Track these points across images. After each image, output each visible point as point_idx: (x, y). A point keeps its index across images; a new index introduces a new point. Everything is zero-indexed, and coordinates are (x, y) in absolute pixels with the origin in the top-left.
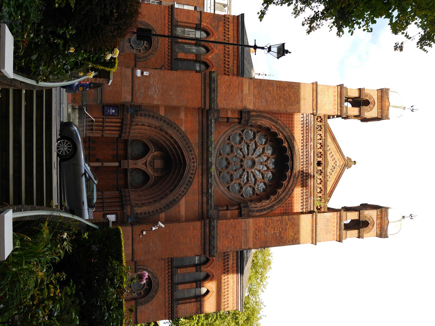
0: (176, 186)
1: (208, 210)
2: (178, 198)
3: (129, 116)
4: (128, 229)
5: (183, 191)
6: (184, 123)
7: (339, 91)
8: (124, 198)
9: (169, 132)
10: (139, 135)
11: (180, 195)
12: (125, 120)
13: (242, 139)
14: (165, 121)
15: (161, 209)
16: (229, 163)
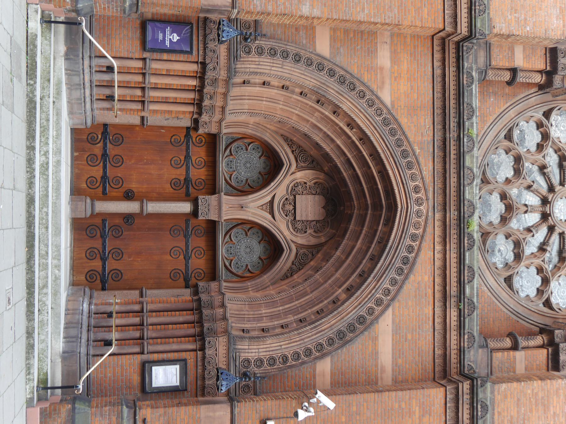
0: (363, 277)
1: (461, 351)
2: (371, 311)
3: (222, 50)
4: (218, 414)
5: (387, 292)
6: (387, 81)
8: (205, 312)
9: (346, 106)
10: (252, 120)
11: (379, 302)
12: (210, 66)
13: (546, 136)
14: (332, 73)
16: (509, 208)
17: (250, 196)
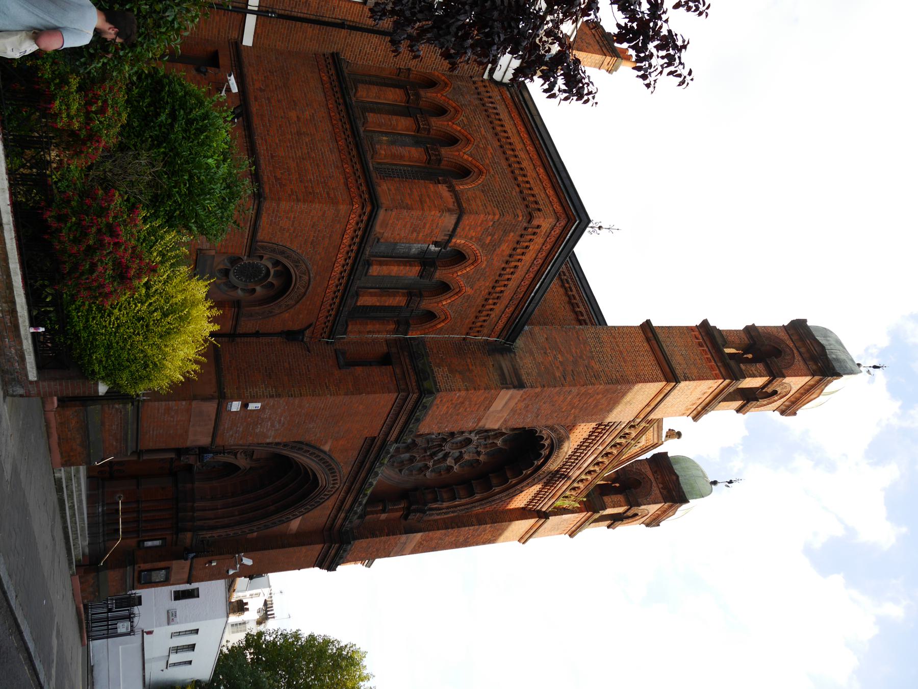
7: (722, 386)
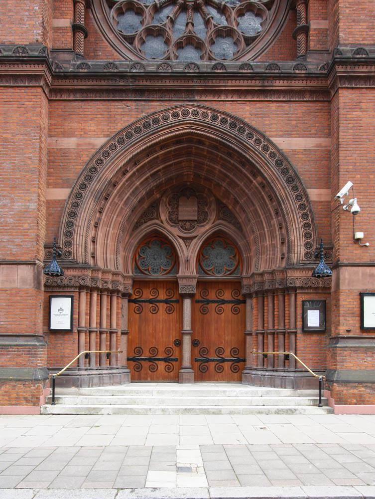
0: (245, 162)
2: (272, 155)
3: (69, 273)
5: (258, 141)
6: (87, 140)
8: (267, 287)
11: (266, 148)
12: (82, 282)
14: (83, 187)
15: (299, 197)
17: (180, 255)
